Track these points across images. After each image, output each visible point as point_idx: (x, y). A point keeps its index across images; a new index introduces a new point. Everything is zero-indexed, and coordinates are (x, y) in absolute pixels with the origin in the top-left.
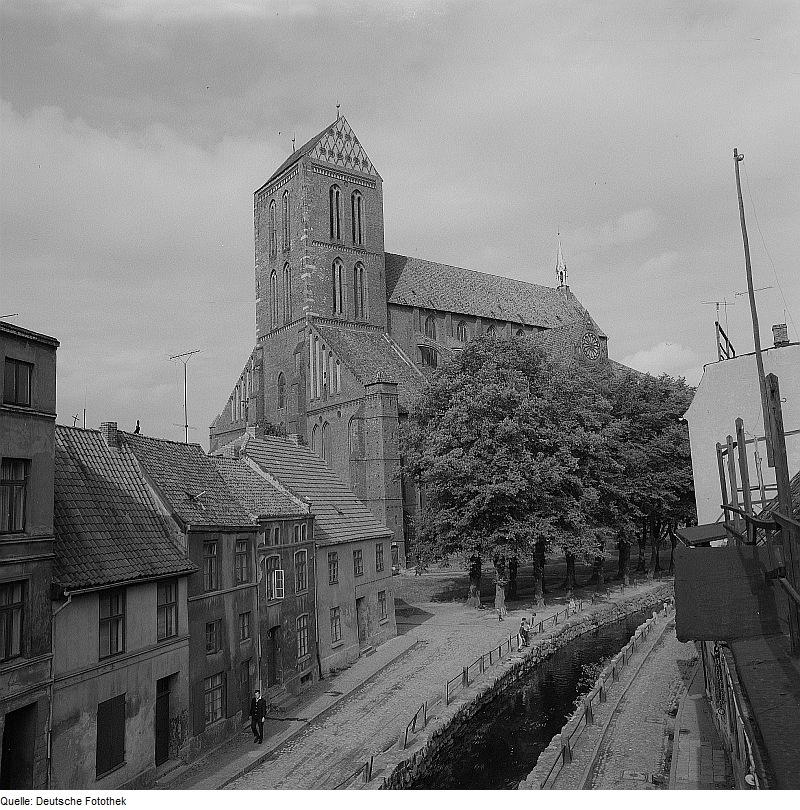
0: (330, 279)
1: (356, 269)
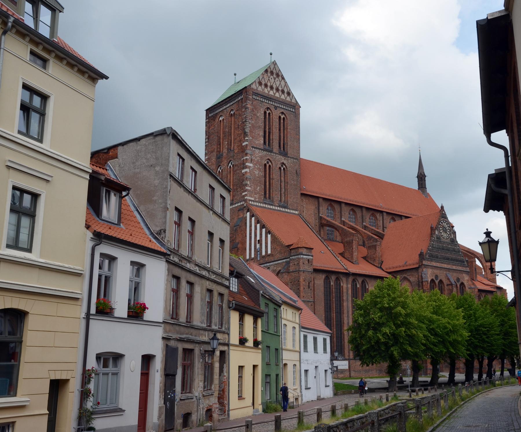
0: (262, 174)
1: (280, 168)
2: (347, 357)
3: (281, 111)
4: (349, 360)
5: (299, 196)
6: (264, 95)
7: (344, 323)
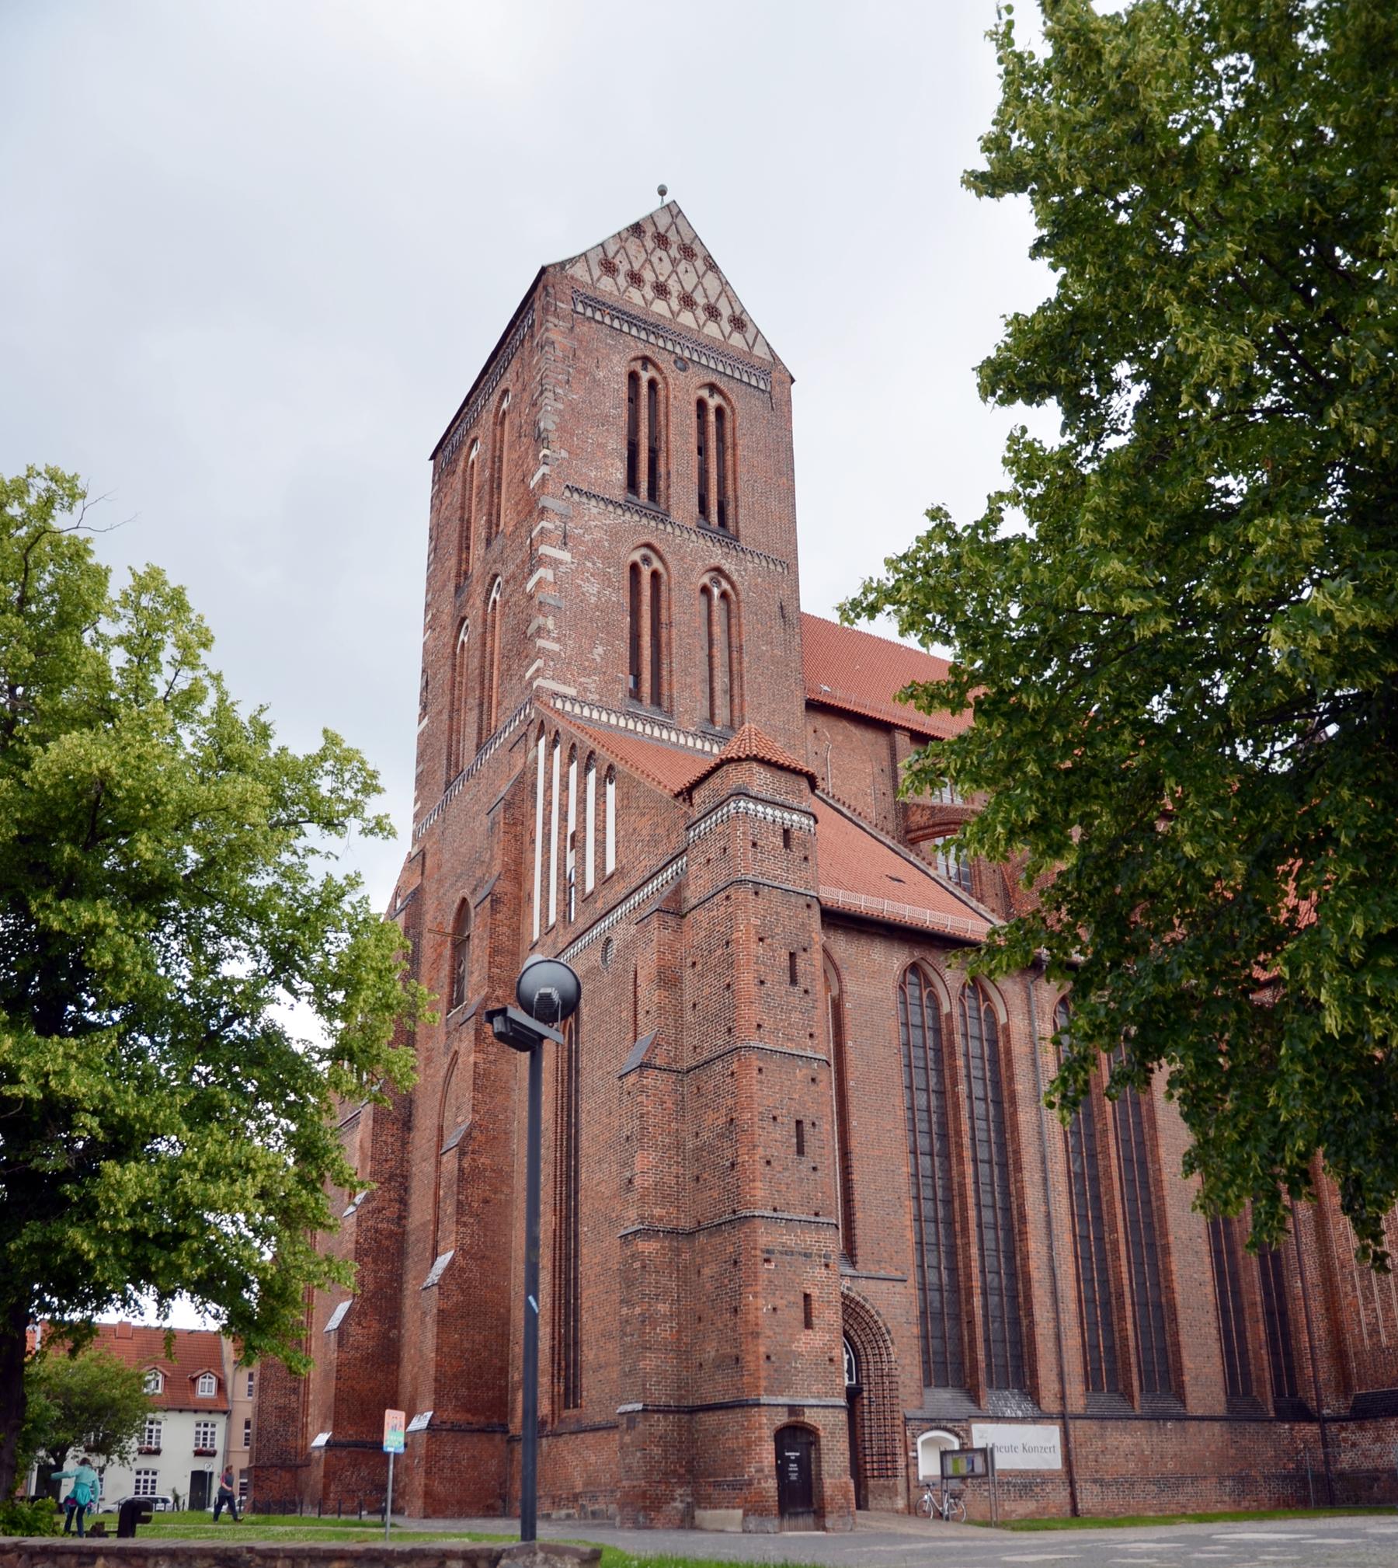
1: (705, 590)
2: (1050, 1403)
3: (707, 380)
4: (1064, 1418)
5: (799, 707)
6: (627, 309)
7: (1023, 1218)
